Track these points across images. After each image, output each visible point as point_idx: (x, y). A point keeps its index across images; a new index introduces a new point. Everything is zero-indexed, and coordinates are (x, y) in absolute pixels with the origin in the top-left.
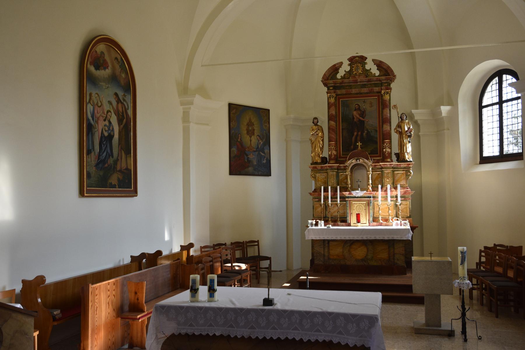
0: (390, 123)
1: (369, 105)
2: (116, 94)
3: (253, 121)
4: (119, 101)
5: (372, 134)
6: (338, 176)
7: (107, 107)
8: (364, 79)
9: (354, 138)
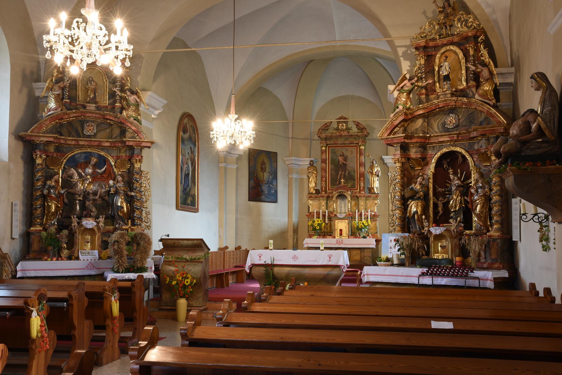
0: (365, 166)
1: (351, 153)
2: (191, 148)
3: (265, 161)
4: (192, 152)
5: (352, 174)
6: (327, 203)
7: (187, 156)
8: (347, 134)
9: (339, 176)
